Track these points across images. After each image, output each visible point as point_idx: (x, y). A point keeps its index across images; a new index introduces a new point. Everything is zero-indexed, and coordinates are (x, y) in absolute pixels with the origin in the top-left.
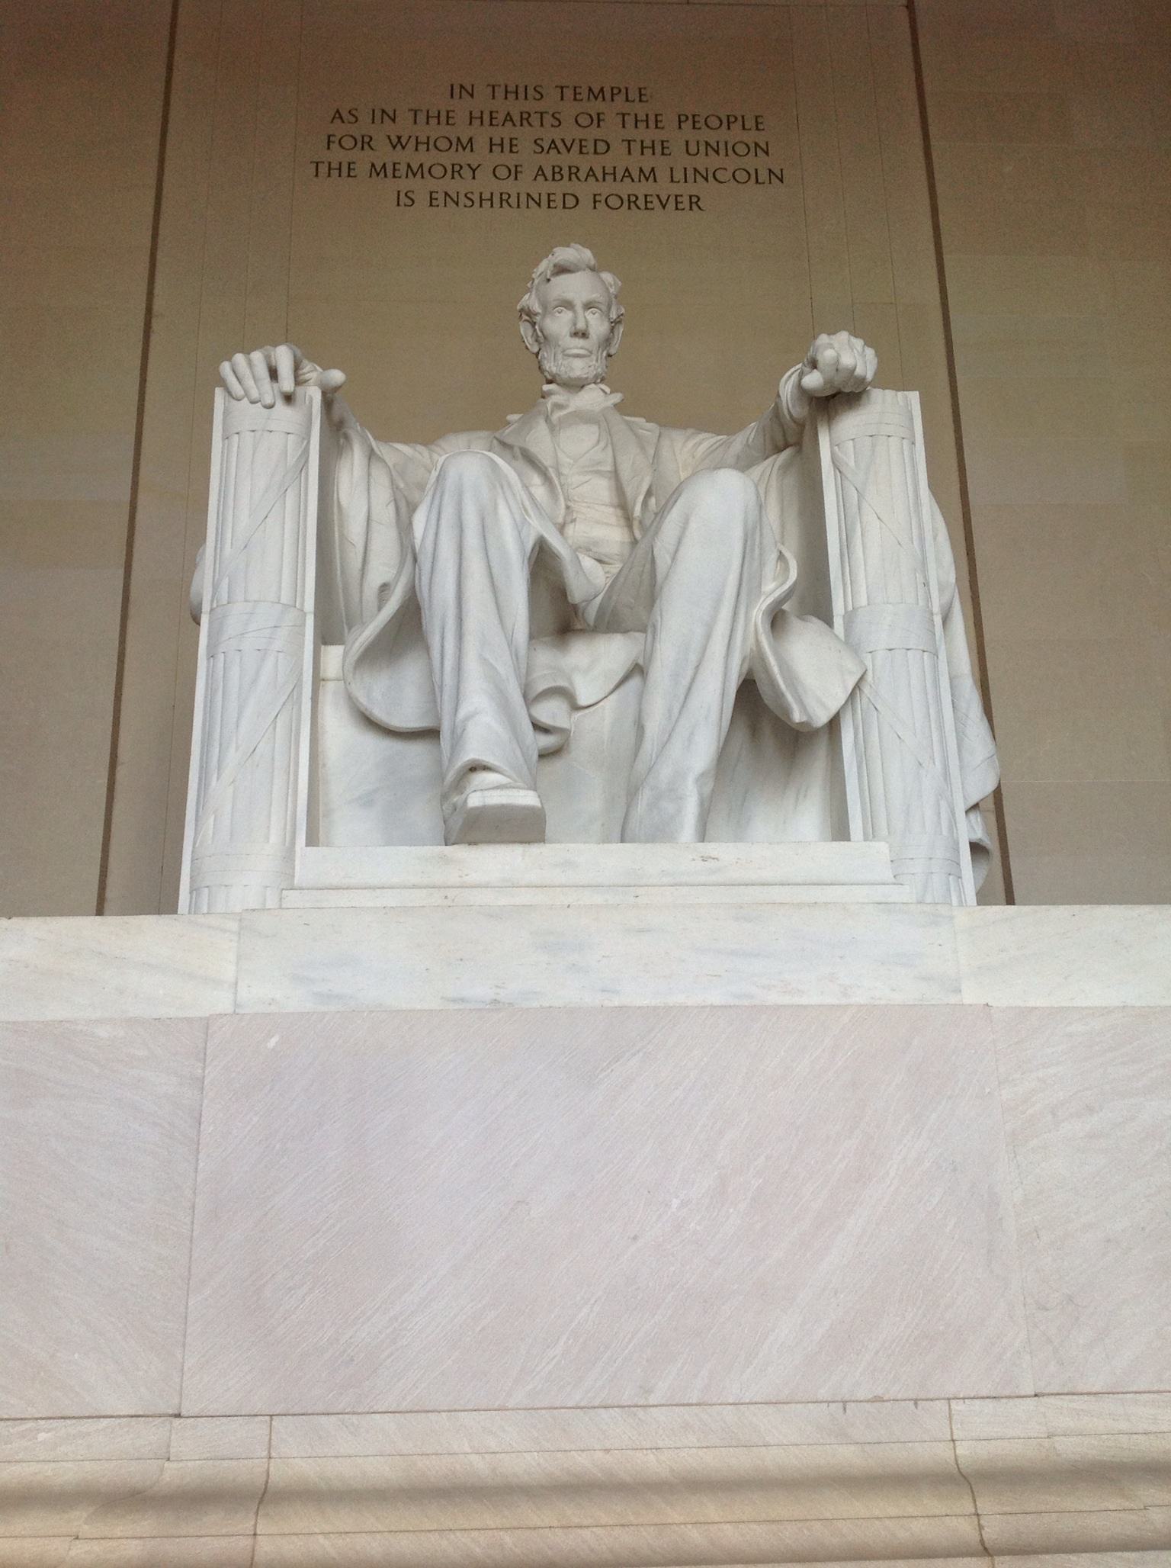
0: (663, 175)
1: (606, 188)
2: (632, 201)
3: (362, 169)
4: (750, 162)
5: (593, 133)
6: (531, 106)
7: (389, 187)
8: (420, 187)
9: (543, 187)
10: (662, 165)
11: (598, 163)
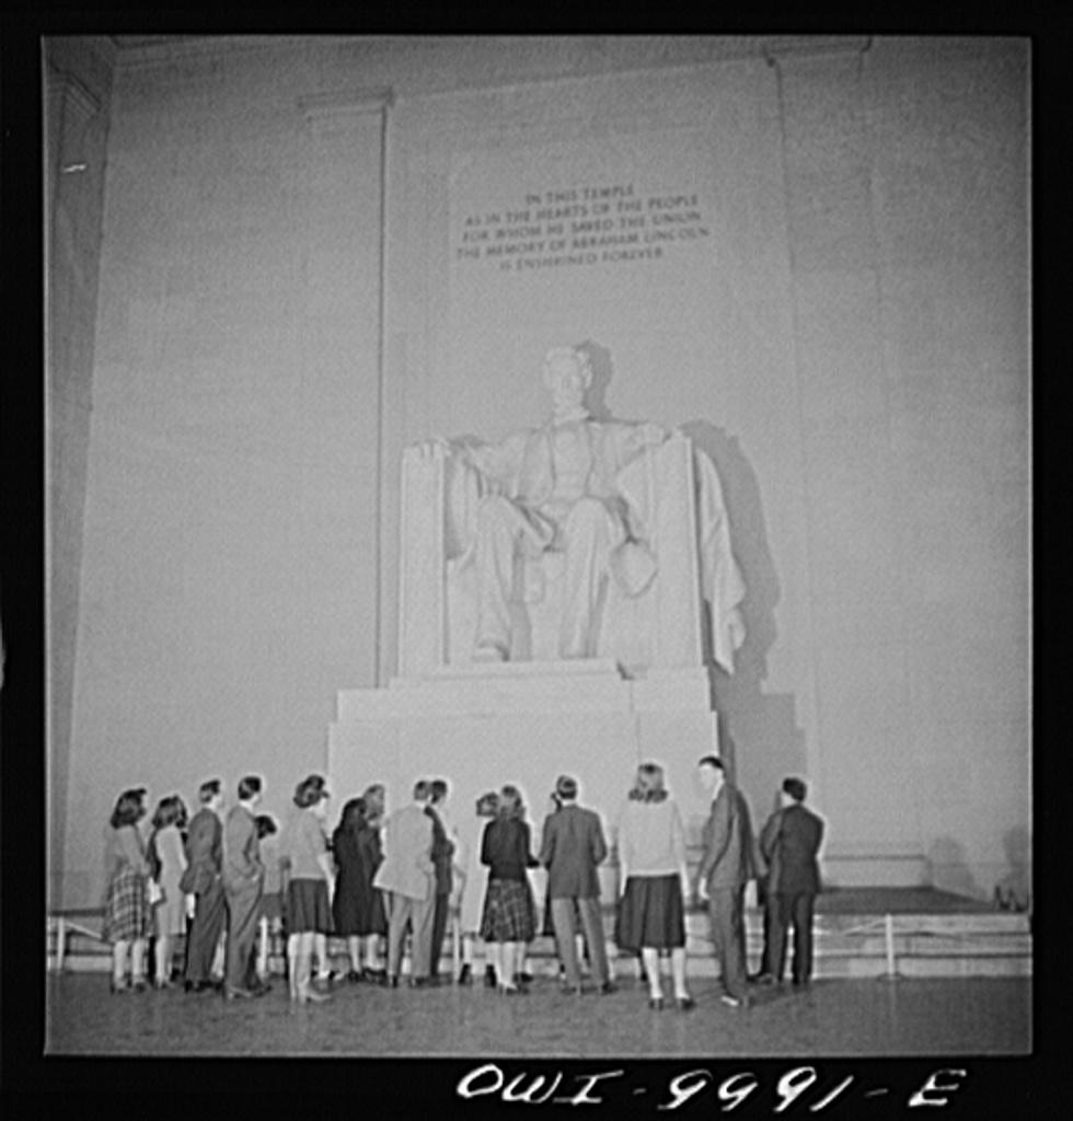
0: (641, 238)
1: (610, 249)
2: (624, 255)
3: (483, 251)
4: (690, 224)
5: (603, 217)
6: (571, 204)
7: (496, 260)
8: (513, 258)
9: (577, 252)
10: (639, 231)
11: (608, 234)
